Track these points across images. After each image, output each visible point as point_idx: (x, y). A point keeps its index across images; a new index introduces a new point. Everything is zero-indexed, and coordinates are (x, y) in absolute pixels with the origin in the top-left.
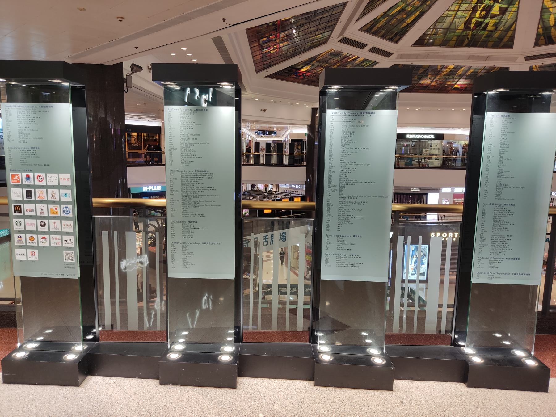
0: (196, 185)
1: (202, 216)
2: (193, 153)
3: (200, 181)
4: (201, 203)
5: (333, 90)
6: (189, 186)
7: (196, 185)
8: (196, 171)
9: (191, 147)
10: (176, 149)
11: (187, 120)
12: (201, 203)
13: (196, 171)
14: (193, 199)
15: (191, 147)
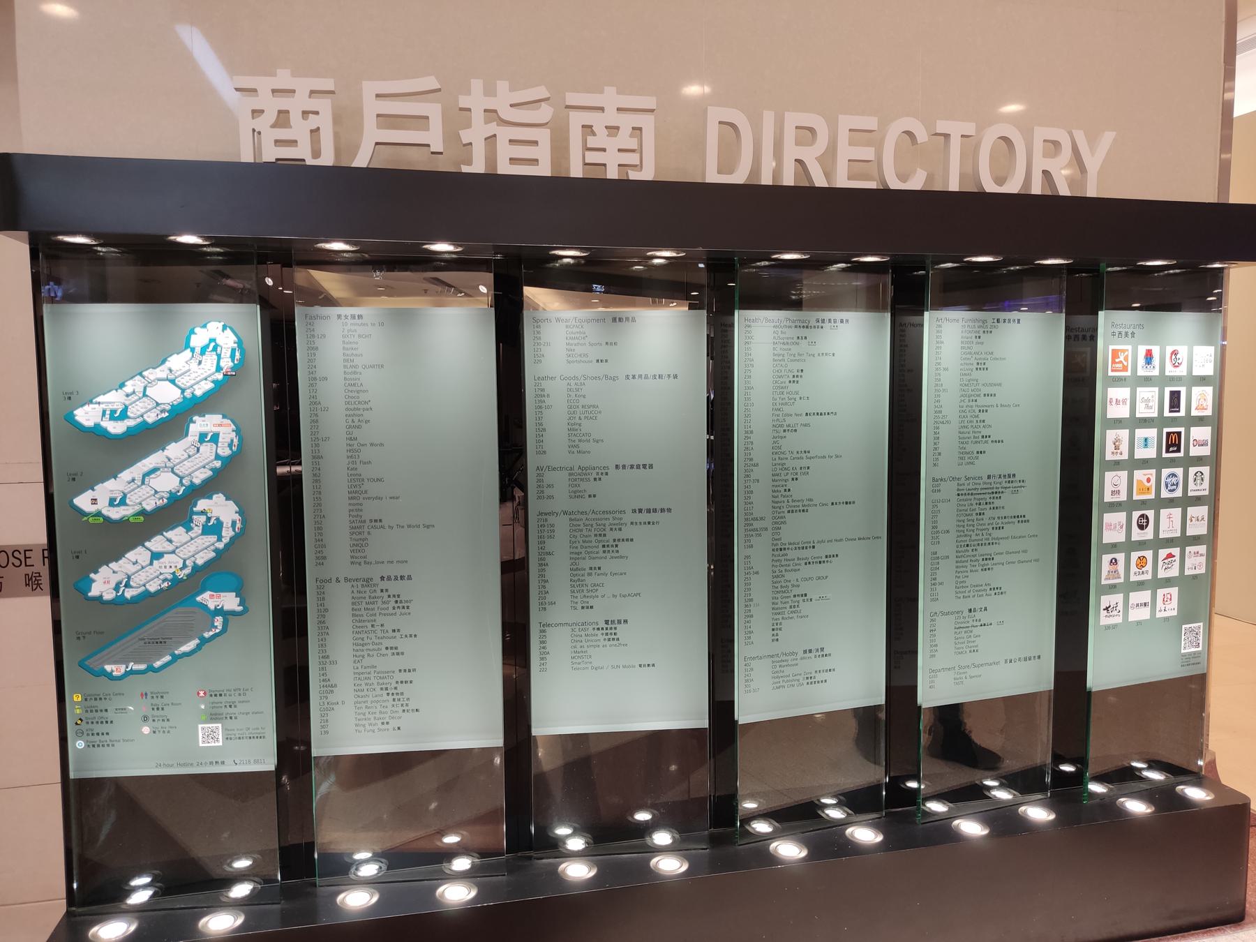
0: (989, 513)
1: (998, 591)
2: (985, 432)
3: (997, 503)
4: (997, 559)
5: (656, 261)
6: (975, 517)
7: (989, 513)
8: (989, 477)
9: (982, 416)
12: (997, 559)
14: (983, 550)
15: (982, 416)
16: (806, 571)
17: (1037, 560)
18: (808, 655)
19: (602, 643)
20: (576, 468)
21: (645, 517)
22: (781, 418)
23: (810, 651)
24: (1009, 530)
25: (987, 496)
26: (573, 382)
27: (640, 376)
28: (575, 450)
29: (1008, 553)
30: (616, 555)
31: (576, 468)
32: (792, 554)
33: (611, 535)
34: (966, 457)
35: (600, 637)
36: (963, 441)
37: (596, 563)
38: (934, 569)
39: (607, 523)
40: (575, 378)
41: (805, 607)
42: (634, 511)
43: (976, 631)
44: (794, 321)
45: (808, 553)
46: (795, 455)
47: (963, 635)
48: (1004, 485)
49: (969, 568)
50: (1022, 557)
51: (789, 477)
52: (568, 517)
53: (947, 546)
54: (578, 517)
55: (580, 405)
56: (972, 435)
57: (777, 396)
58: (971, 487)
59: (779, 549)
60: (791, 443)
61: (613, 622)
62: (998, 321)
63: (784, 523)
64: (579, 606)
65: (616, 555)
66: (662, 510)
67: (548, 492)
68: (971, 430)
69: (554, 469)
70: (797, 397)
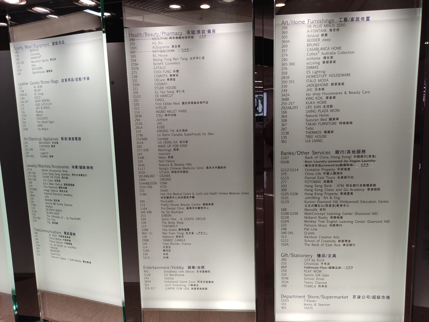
0: (336, 181)
1: (347, 243)
2: (333, 115)
3: (345, 173)
4: (345, 218)
6: (322, 183)
7: (336, 181)
9: (329, 102)
10: (295, 107)
11: (322, 44)
13: (337, 152)
14: (329, 210)
15: (329, 102)
16: (188, 213)
17: (388, 222)
18: (191, 270)
19: (64, 245)
20: (42, 139)
21: (78, 171)
22: (162, 106)
23: (193, 267)
24: (357, 196)
25: (336, 168)
26: (36, 86)
27: (69, 79)
28: (41, 128)
29: (356, 214)
30: (66, 193)
31: (42, 139)
32: (176, 201)
33: (63, 181)
34: (311, 134)
35: (62, 241)
36: (310, 123)
37: (57, 197)
38: (285, 221)
39: (60, 173)
40: (37, 83)
41: (187, 238)
42: (73, 167)
43: (325, 272)
44: (168, 34)
45: (190, 201)
46: (175, 133)
47: (312, 273)
48: (353, 159)
49: (317, 223)
50: (372, 218)
51: (172, 148)
52: (41, 168)
53: (298, 204)
54: (46, 169)
55: (41, 99)
56: (319, 118)
57: (158, 90)
58: (318, 159)
59: (167, 197)
60: (171, 123)
61: (68, 233)
62: (346, 20)
63: (170, 179)
64: (51, 221)
65: (66, 193)
66: (88, 167)
67: (31, 153)
68: (318, 114)
69: (32, 139)
70: (175, 90)
